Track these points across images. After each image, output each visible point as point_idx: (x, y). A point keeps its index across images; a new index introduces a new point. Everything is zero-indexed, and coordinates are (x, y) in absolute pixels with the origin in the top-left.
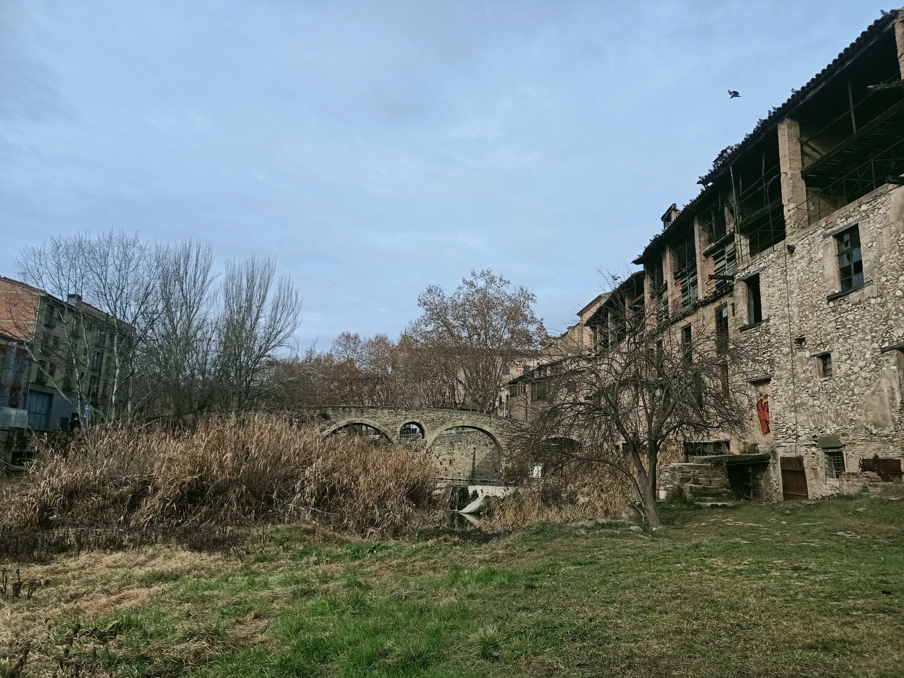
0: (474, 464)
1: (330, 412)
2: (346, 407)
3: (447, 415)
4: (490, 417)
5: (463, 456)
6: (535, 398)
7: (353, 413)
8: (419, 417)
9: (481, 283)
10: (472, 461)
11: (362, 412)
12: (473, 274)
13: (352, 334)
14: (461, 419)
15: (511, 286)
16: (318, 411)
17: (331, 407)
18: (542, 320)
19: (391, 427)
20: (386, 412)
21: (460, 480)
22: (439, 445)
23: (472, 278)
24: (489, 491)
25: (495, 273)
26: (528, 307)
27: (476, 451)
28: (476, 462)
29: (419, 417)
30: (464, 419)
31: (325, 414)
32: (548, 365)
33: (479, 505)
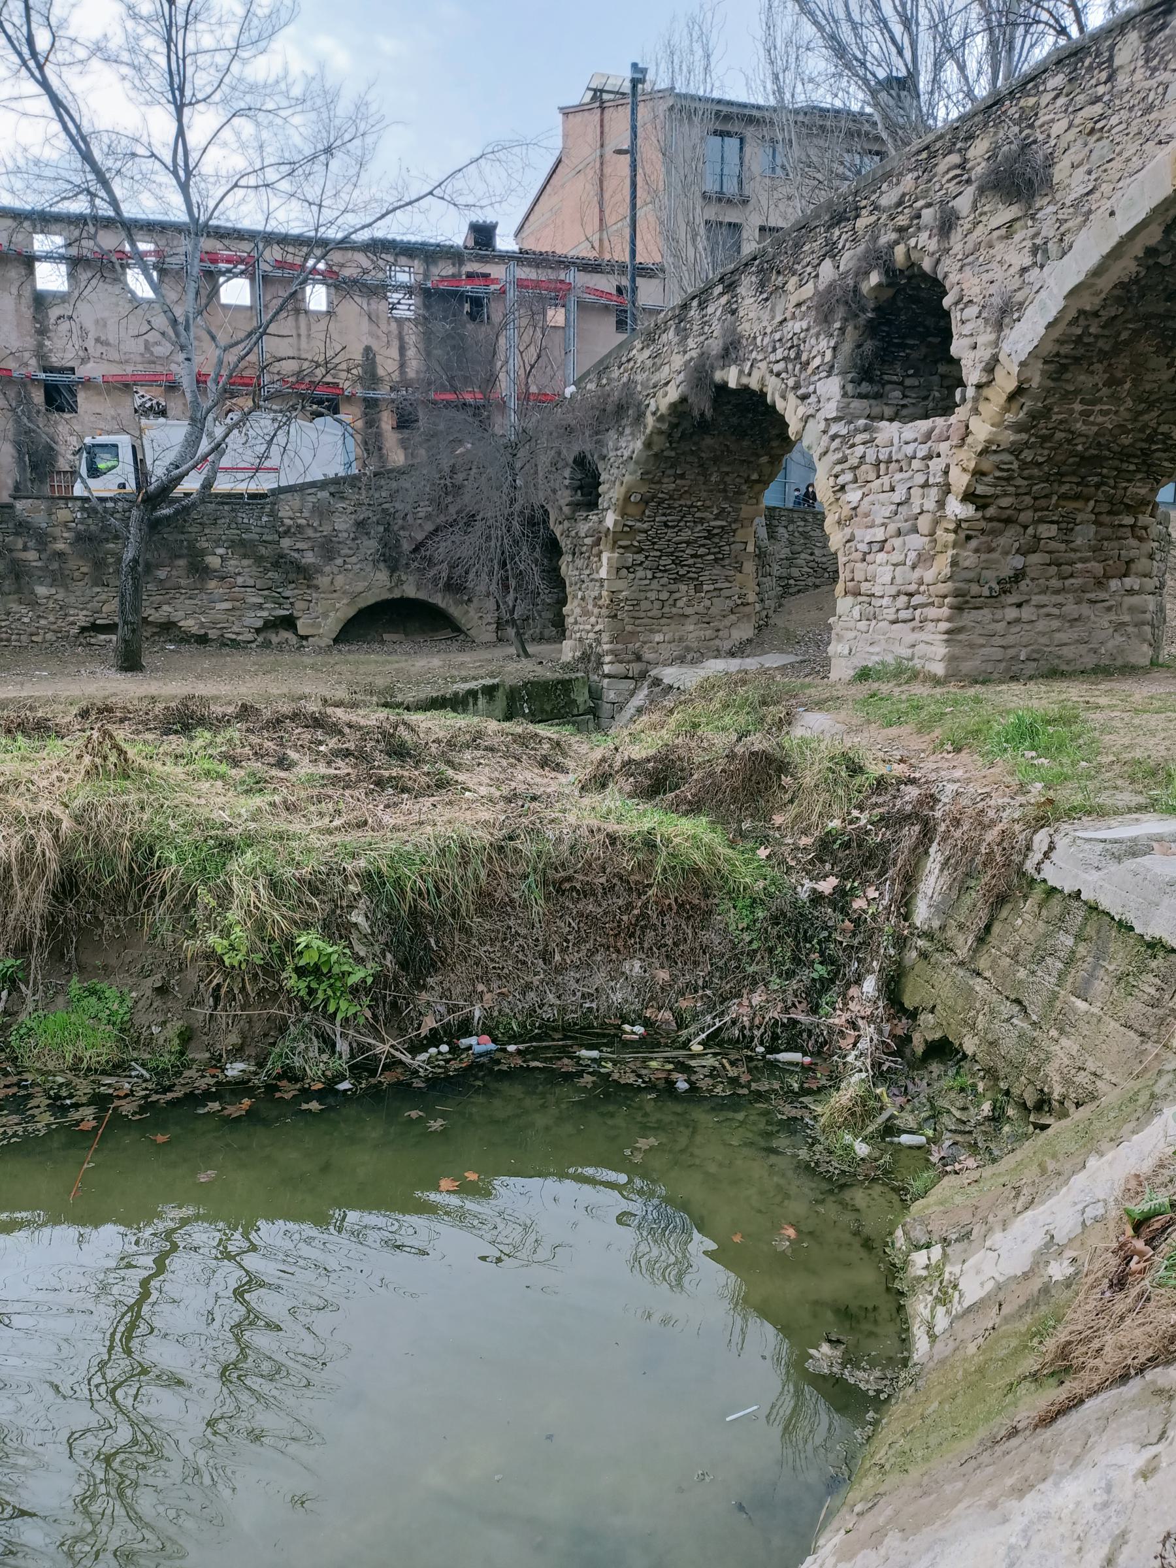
16: (979, 149)
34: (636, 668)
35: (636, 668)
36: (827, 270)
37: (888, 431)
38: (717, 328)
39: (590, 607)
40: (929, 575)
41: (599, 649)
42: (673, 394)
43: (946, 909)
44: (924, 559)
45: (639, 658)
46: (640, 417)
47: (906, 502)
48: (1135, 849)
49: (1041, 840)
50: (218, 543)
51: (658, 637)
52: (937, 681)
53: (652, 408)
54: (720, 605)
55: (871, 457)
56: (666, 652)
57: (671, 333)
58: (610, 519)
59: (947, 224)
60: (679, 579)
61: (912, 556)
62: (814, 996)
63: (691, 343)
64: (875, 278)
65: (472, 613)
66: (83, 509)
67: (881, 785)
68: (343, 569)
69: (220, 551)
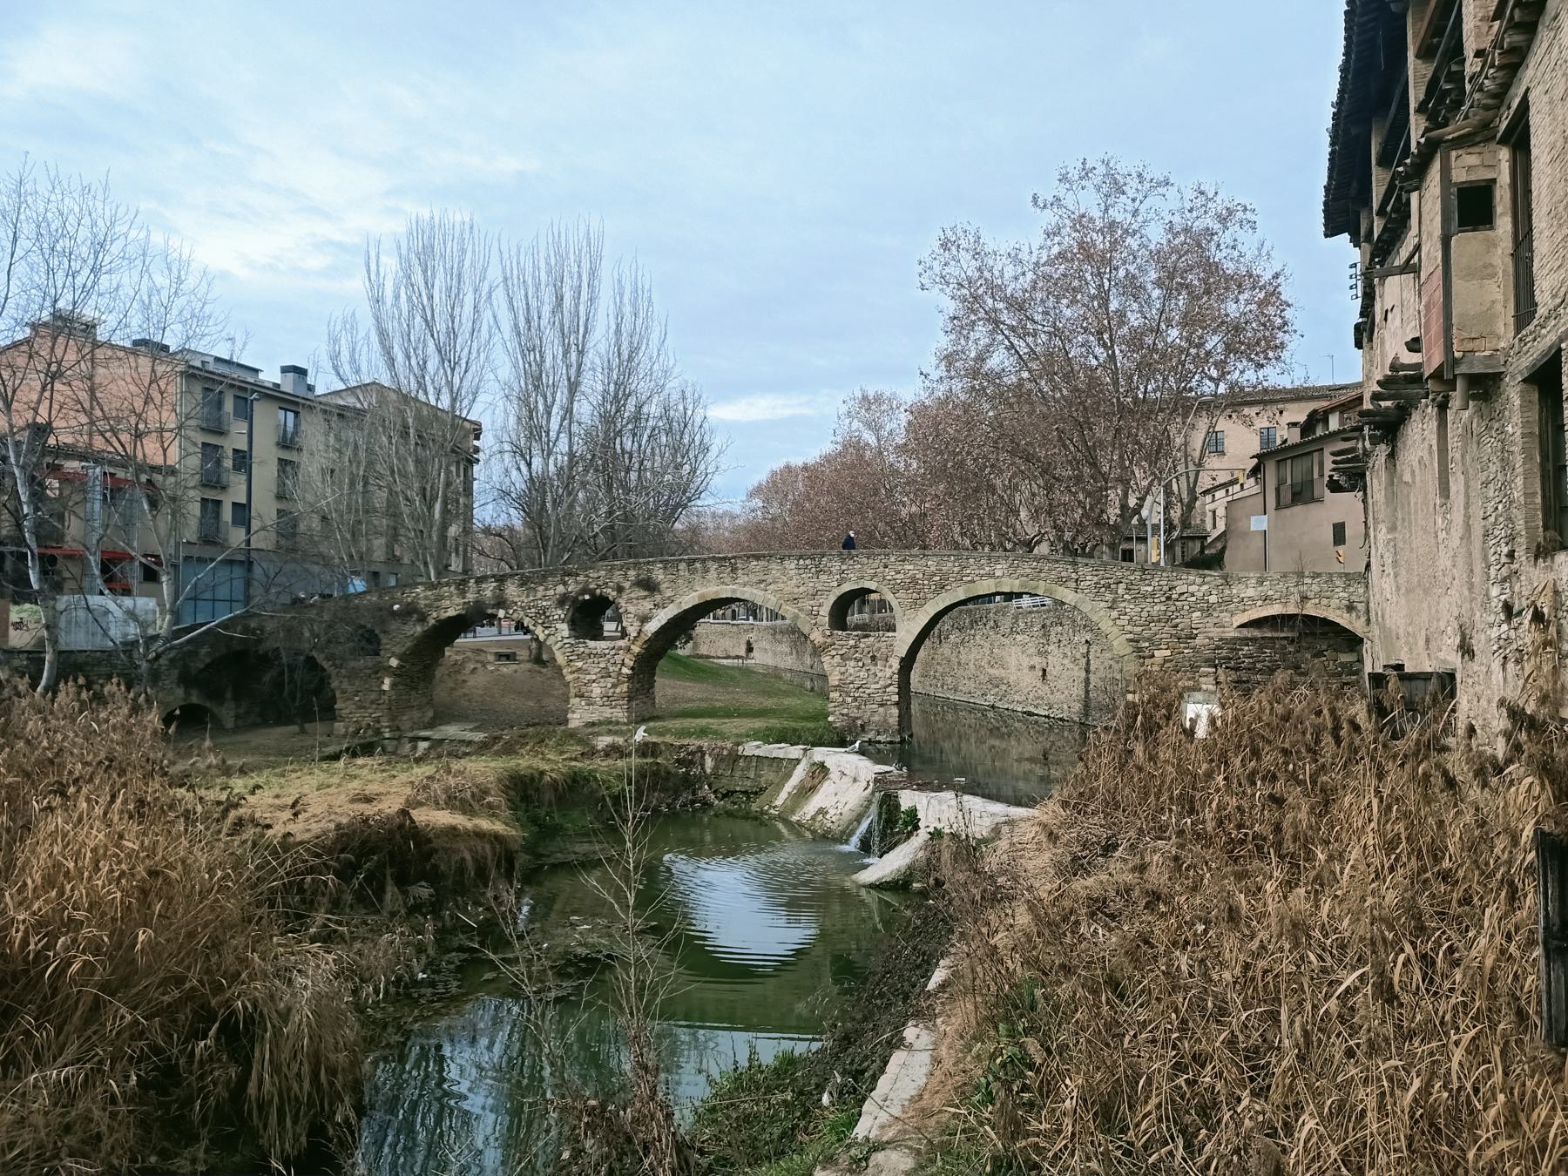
0: (1087, 682)
1: (659, 575)
2: (695, 560)
3: (950, 566)
4: (1075, 564)
5: (1066, 661)
6: (1287, 496)
7: (713, 574)
8: (875, 575)
9: (1089, 202)
10: (1083, 674)
11: (734, 570)
12: (1064, 179)
13: (871, 394)
14: (991, 576)
15: (1171, 192)
16: (632, 573)
17: (661, 562)
18: (1276, 276)
19: (807, 604)
20: (793, 566)
21: (1062, 719)
22: (1023, 632)
23: (1061, 191)
24: (943, 819)
25: (1125, 165)
26: (1234, 248)
27: (1094, 648)
28: (1092, 677)
29: (875, 575)
30: (998, 573)
31: (649, 578)
32: (1332, 410)
33: (908, 861)
34: (397, 734)
35: (397, 734)
36: (561, 589)
37: (591, 644)
38: (488, 593)
39: (367, 705)
40: (618, 690)
41: (377, 726)
42: (451, 613)
43: (715, 768)
44: (614, 686)
45: (398, 729)
46: (423, 618)
47: (606, 668)
48: (758, 747)
49: (740, 748)
50: (100, 676)
51: (405, 718)
52: (625, 724)
53: (435, 615)
54: (425, 700)
55: (587, 651)
56: (407, 726)
57: (452, 589)
58: (394, 662)
59: (620, 589)
60: (413, 688)
61: (609, 685)
62: (694, 794)
63: (468, 595)
64: (587, 597)
65: (224, 712)
66: (28, 659)
67: (680, 747)
68: (163, 689)
69: (101, 681)
